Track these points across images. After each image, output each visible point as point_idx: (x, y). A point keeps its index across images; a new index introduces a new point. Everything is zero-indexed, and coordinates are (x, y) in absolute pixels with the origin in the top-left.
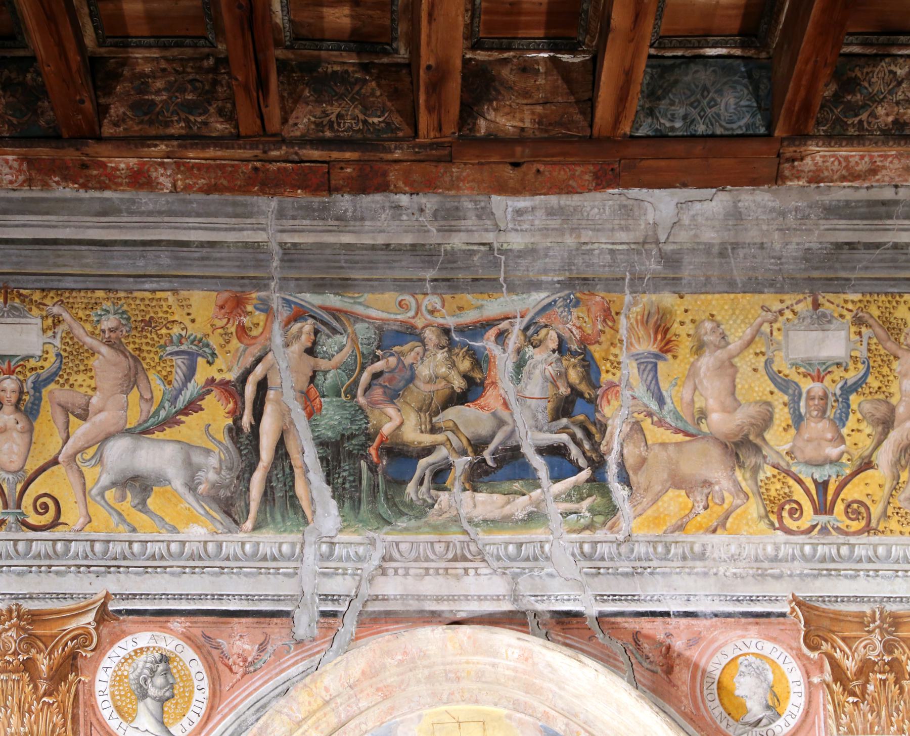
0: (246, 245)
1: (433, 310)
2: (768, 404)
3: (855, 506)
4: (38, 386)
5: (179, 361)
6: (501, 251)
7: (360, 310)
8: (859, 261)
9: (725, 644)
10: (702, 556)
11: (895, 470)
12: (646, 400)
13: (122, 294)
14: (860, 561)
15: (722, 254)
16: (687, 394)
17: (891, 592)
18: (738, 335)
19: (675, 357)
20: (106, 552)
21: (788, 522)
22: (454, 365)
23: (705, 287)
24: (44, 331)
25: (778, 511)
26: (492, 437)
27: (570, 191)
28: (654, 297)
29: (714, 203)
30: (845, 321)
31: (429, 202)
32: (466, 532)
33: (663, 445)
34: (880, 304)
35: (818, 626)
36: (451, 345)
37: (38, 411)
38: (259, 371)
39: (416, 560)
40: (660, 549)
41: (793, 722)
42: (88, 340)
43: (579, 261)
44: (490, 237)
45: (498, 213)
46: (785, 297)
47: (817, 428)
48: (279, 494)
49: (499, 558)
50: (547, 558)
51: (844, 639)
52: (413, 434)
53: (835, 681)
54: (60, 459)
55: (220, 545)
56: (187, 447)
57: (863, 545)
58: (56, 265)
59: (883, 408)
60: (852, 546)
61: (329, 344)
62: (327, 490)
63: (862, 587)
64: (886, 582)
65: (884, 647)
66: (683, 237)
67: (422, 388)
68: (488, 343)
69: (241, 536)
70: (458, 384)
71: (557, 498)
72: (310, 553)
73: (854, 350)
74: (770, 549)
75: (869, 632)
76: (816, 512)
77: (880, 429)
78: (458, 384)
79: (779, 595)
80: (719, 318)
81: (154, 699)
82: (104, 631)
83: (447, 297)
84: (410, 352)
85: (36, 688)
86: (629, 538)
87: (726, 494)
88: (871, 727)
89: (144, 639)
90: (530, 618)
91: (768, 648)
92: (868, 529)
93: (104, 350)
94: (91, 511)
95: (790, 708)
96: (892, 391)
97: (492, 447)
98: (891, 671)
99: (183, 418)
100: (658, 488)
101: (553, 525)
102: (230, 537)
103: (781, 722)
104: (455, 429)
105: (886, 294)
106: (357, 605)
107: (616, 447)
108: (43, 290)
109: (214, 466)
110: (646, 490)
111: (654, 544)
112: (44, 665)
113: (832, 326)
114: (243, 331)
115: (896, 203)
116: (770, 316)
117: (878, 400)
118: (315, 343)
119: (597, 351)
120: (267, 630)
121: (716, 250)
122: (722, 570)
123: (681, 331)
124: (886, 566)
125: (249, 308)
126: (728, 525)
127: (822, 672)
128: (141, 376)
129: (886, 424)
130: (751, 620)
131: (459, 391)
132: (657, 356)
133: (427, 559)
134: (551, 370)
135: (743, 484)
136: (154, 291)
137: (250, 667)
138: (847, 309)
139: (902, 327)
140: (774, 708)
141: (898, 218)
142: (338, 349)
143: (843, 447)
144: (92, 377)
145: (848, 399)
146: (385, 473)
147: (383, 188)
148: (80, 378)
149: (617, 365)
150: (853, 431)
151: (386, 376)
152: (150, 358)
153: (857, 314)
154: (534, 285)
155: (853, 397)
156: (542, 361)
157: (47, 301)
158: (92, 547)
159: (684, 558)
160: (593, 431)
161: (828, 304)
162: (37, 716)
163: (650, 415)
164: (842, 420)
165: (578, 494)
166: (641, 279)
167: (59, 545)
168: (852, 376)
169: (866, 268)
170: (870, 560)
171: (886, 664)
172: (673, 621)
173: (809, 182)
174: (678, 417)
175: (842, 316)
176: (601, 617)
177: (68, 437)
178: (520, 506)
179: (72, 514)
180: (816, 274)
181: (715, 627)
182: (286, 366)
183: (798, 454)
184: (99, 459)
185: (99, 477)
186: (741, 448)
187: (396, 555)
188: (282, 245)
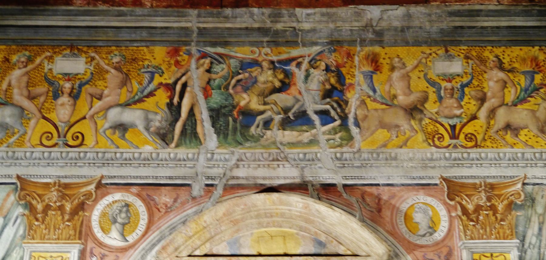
0: (182, 28)
1: (266, 54)
2: (426, 92)
3: (469, 135)
4: (80, 86)
5: (147, 75)
6: (299, 30)
7: (232, 54)
8: (466, 33)
9: (407, 198)
10: (395, 159)
12: (367, 91)
13: (124, 48)
14: (473, 160)
15: (402, 30)
16: (387, 88)
17: (489, 174)
18: (410, 64)
19: (381, 73)
20: (103, 157)
21: (437, 143)
22: (276, 76)
23: (395, 44)
24: (86, 63)
25: (432, 138)
26: (293, 107)
27: (332, 6)
28: (371, 48)
29: (398, 11)
31: (267, 11)
32: (279, 148)
33: (376, 110)
35: (454, 189)
36: (274, 69)
37: (79, 96)
38: (184, 79)
39: (254, 160)
40: (375, 155)
41: (443, 235)
42: (106, 67)
43: (336, 34)
44: (294, 25)
45: (299, 15)
46: (432, 48)
47: (450, 102)
48: (189, 132)
49: (295, 160)
50: (319, 160)
51: (467, 195)
52: (255, 105)
53: (463, 214)
54: (87, 117)
55: (158, 154)
56: (147, 111)
57: (474, 153)
58: (96, 37)
60: (469, 153)
61: (217, 68)
62: (212, 130)
63: (475, 171)
64: (486, 169)
66: (384, 24)
67: (260, 86)
68: (292, 67)
69: (169, 150)
70: (278, 84)
71: (324, 133)
72: (202, 158)
73: (466, 69)
74: (429, 155)
75: (479, 192)
76: (451, 138)
77: (479, 102)
78: (278, 84)
79: (434, 176)
80: (401, 57)
81: (120, 223)
82: (99, 192)
83: (274, 49)
84: (255, 71)
85: (63, 218)
86: (359, 151)
87: (407, 131)
88: (482, 236)
89: (118, 196)
90: (310, 187)
91: (429, 200)
92: (476, 146)
93: (113, 71)
94: (99, 139)
95: (441, 228)
96: (484, 86)
97: (293, 111)
98: (491, 210)
99: (146, 99)
100: (373, 128)
101: (321, 145)
102: (164, 151)
103: (436, 234)
104: (275, 104)
105: (479, 46)
106: (224, 181)
107: (353, 110)
108: (88, 46)
109: (159, 120)
110: (368, 129)
111: (372, 153)
112: (68, 207)
113: (455, 60)
114: (177, 63)
115: (481, 11)
116: (425, 56)
117: (478, 90)
118: (211, 68)
119: (344, 70)
120: (179, 192)
121: (399, 29)
122: (405, 165)
123: (384, 62)
124: (486, 162)
125: (181, 53)
126: (408, 144)
127: (456, 210)
128: (128, 82)
129: (482, 100)
130: (420, 187)
131: (277, 87)
132: (372, 72)
133: (259, 160)
134: (322, 78)
135: (415, 127)
136: (138, 47)
137: (168, 209)
140: (432, 229)
141: (482, 16)
142: (221, 70)
143: (462, 110)
144: (106, 82)
146: (241, 122)
147: (247, 5)
148: (100, 83)
149: (353, 76)
151: (244, 81)
152: (133, 74)
154: (315, 44)
155: (466, 89)
156: (318, 75)
157: (90, 51)
158: (97, 155)
159: (387, 159)
160: (343, 104)
162: (62, 231)
163: (369, 97)
164: (462, 98)
165: (334, 131)
166: (365, 41)
167: (82, 155)
168: (465, 80)
169: (469, 36)
170: (478, 160)
172: (381, 188)
173: (441, 2)
174: (383, 98)
175: (459, 55)
176: (345, 186)
177: (92, 107)
178: (306, 137)
179: (90, 140)
180: (446, 39)
181: (402, 190)
182: (196, 76)
183: (441, 113)
184: (105, 117)
185: (104, 125)
186: (414, 111)
187: (244, 158)
188: (198, 28)
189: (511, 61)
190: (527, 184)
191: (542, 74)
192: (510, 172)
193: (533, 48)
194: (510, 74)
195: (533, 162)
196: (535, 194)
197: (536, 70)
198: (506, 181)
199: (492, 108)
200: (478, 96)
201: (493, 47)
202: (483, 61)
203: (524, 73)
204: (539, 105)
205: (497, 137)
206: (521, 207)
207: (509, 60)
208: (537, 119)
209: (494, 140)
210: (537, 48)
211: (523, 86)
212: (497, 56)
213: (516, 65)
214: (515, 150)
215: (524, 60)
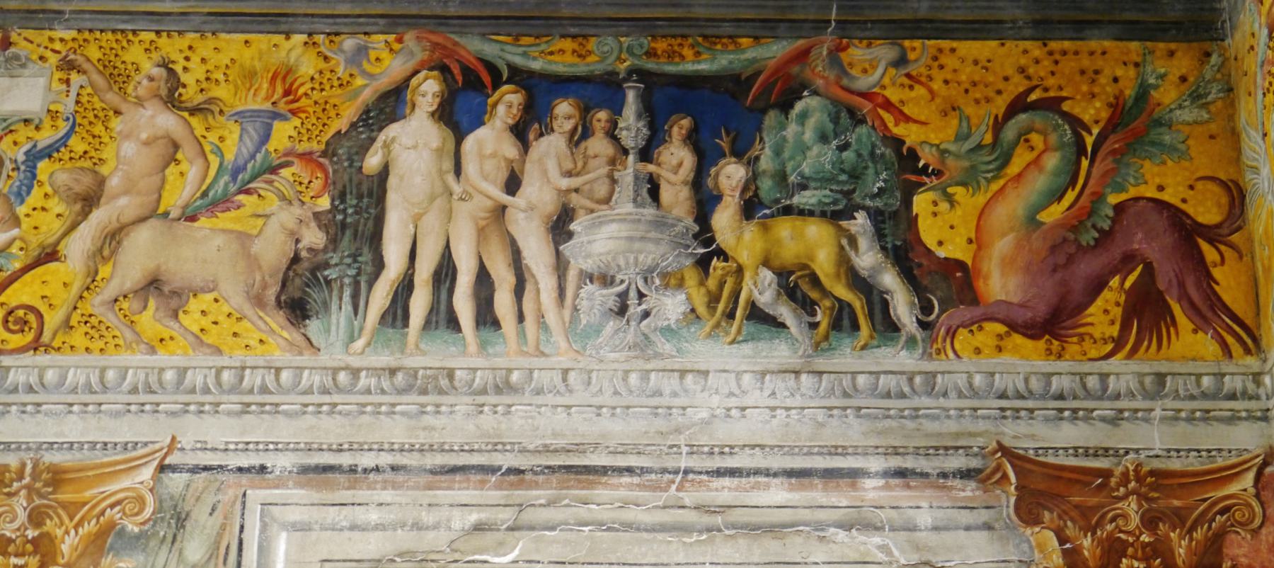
3: (21, 313)
11: (91, 264)
17: (56, 435)
30: (47, 65)
34: (103, 44)
57: (21, 369)
59: (87, 181)
65: (30, 516)
73: (54, 102)
75: (10, 495)
77: (78, 207)
92: (35, 346)
96: (104, 157)
98: (35, 552)
113: (26, 72)
117: (82, 169)
124: (55, 398)
129: (89, 201)
138: (54, 51)
139: (133, 74)
143: (15, 232)
145: (35, 167)
150: (34, 209)
153: (66, 56)
155: (43, 166)
161: (25, 43)
168: (46, 137)
170: (30, 389)
171: (28, 541)
189: (208, 79)
190: (173, 468)
191: (297, 122)
192: (124, 430)
193: (288, 38)
194: (194, 121)
195: (209, 398)
196: (190, 500)
197: (282, 107)
198: (106, 460)
199: (115, 225)
200: (78, 188)
201: (158, 32)
202: (116, 76)
203: (240, 116)
204: (267, 216)
205: (111, 319)
206: (138, 542)
207: (202, 77)
208: (252, 262)
209: (94, 327)
210: (299, 39)
211: (229, 157)
212: (166, 65)
213: (221, 92)
214: (161, 358)
215: (250, 75)
